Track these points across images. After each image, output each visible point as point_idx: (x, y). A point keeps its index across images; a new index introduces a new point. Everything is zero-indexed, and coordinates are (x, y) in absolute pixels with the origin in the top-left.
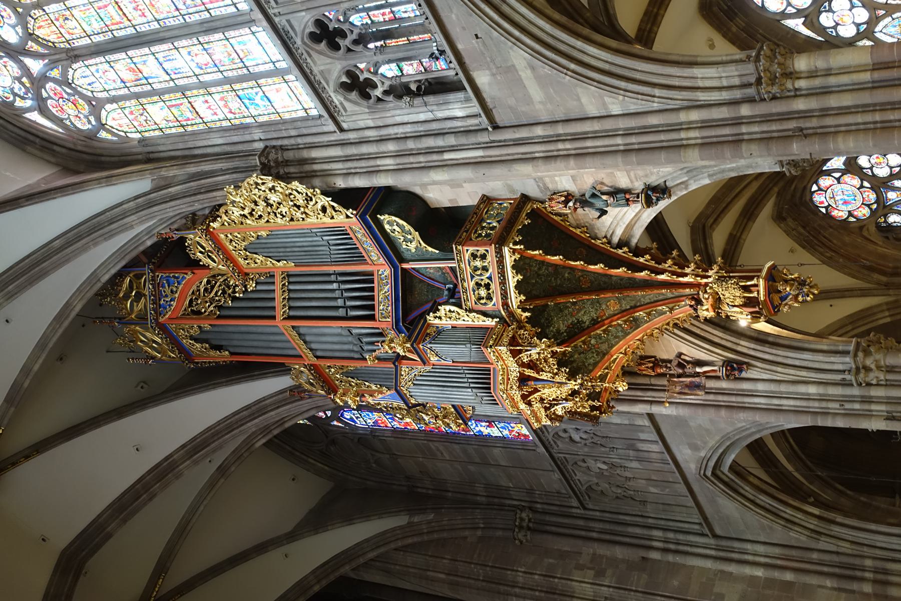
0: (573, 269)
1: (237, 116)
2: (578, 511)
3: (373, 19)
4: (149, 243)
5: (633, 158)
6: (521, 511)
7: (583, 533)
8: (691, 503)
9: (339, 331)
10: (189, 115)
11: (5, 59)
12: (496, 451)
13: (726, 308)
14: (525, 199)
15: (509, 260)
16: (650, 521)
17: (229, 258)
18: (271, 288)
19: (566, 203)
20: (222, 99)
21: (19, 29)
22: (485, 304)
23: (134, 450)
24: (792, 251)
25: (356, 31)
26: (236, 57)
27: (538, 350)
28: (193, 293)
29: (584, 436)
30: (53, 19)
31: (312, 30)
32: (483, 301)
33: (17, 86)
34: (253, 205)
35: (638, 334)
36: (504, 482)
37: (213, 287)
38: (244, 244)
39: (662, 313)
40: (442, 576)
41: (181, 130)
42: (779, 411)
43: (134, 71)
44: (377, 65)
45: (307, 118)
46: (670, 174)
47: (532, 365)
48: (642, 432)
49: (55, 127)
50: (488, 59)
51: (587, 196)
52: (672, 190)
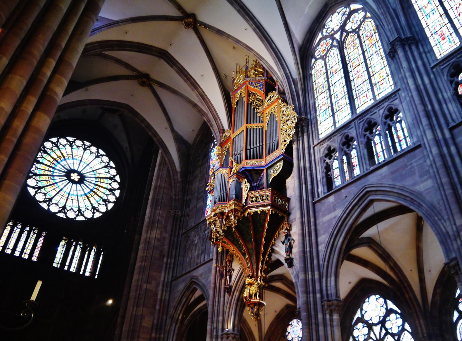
0: (263, 232)
1: (320, 109)
2: (181, 232)
3: (354, 158)
4: (274, 78)
5: (302, 255)
6: (181, 212)
7: (173, 234)
8: (184, 272)
9: (242, 147)
10: (320, 92)
11: (340, 25)
12: (202, 203)
13: (249, 288)
14: (289, 214)
15: (265, 209)
16: (177, 258)
17: (269, 106)
18: (258, 122)
19: (287, 229)
20: (326, 103)
21: (351, 30)
22: (250, 200)
23: (202, 74)
24: (276, 311)
25: (349, 152)
26: (340, 108)
27: (233, 219)
28: (256, 94)
29: (206, 235)
30: (354, 42)
31: (350, 136)
32: (251, 199)
33: (330, 30)
34: (287, 115)
35: (240, 255)
36: (191, 206)
37: (259, 101)
38: (273, 112)
39: (248, 264)
40: (159, 184)
41: (315, 89)
42: (213, 305)
43: (336, 71)
44: (337, 159)
45: (318, 134)
46: (297, 268)
47: (228, 217)
48: (208, 256)
49: (316, 43)
50: (338, 201)
51: (289, 237)
52: (291, 268)
